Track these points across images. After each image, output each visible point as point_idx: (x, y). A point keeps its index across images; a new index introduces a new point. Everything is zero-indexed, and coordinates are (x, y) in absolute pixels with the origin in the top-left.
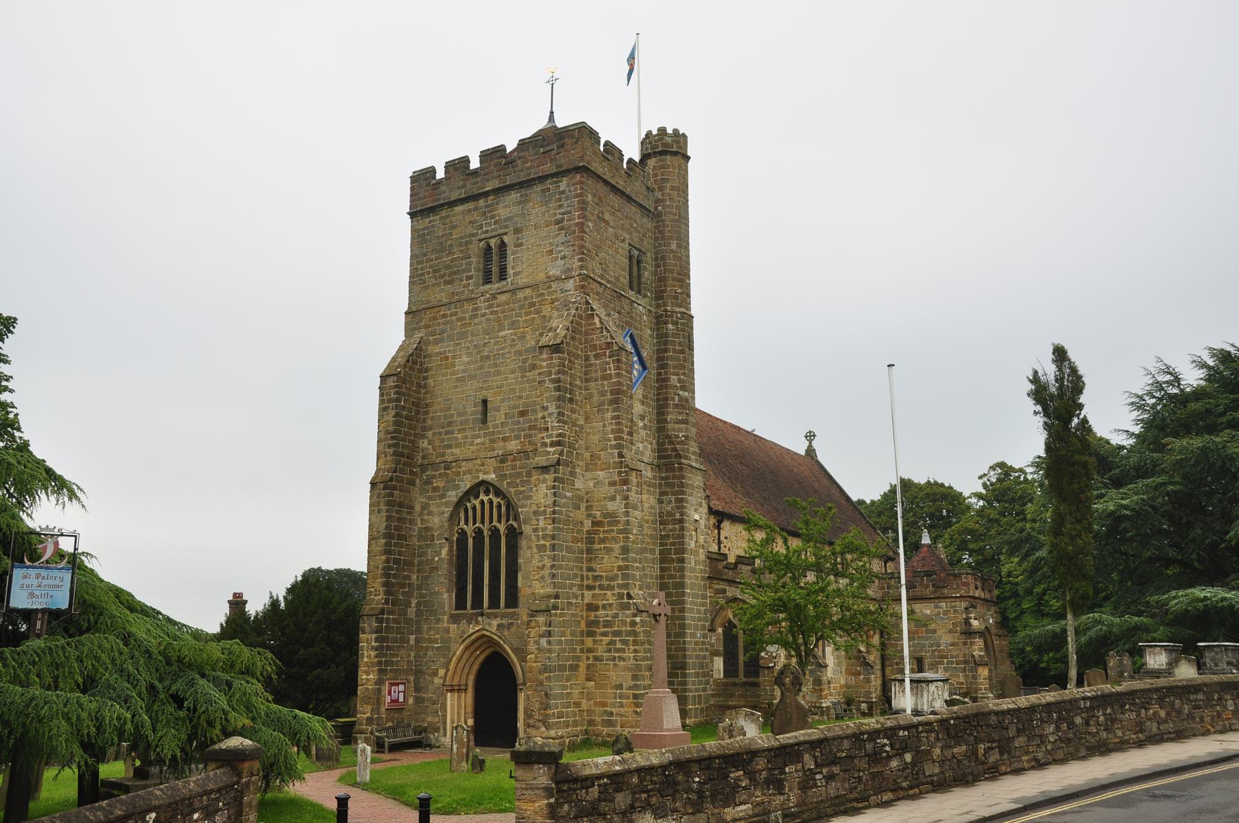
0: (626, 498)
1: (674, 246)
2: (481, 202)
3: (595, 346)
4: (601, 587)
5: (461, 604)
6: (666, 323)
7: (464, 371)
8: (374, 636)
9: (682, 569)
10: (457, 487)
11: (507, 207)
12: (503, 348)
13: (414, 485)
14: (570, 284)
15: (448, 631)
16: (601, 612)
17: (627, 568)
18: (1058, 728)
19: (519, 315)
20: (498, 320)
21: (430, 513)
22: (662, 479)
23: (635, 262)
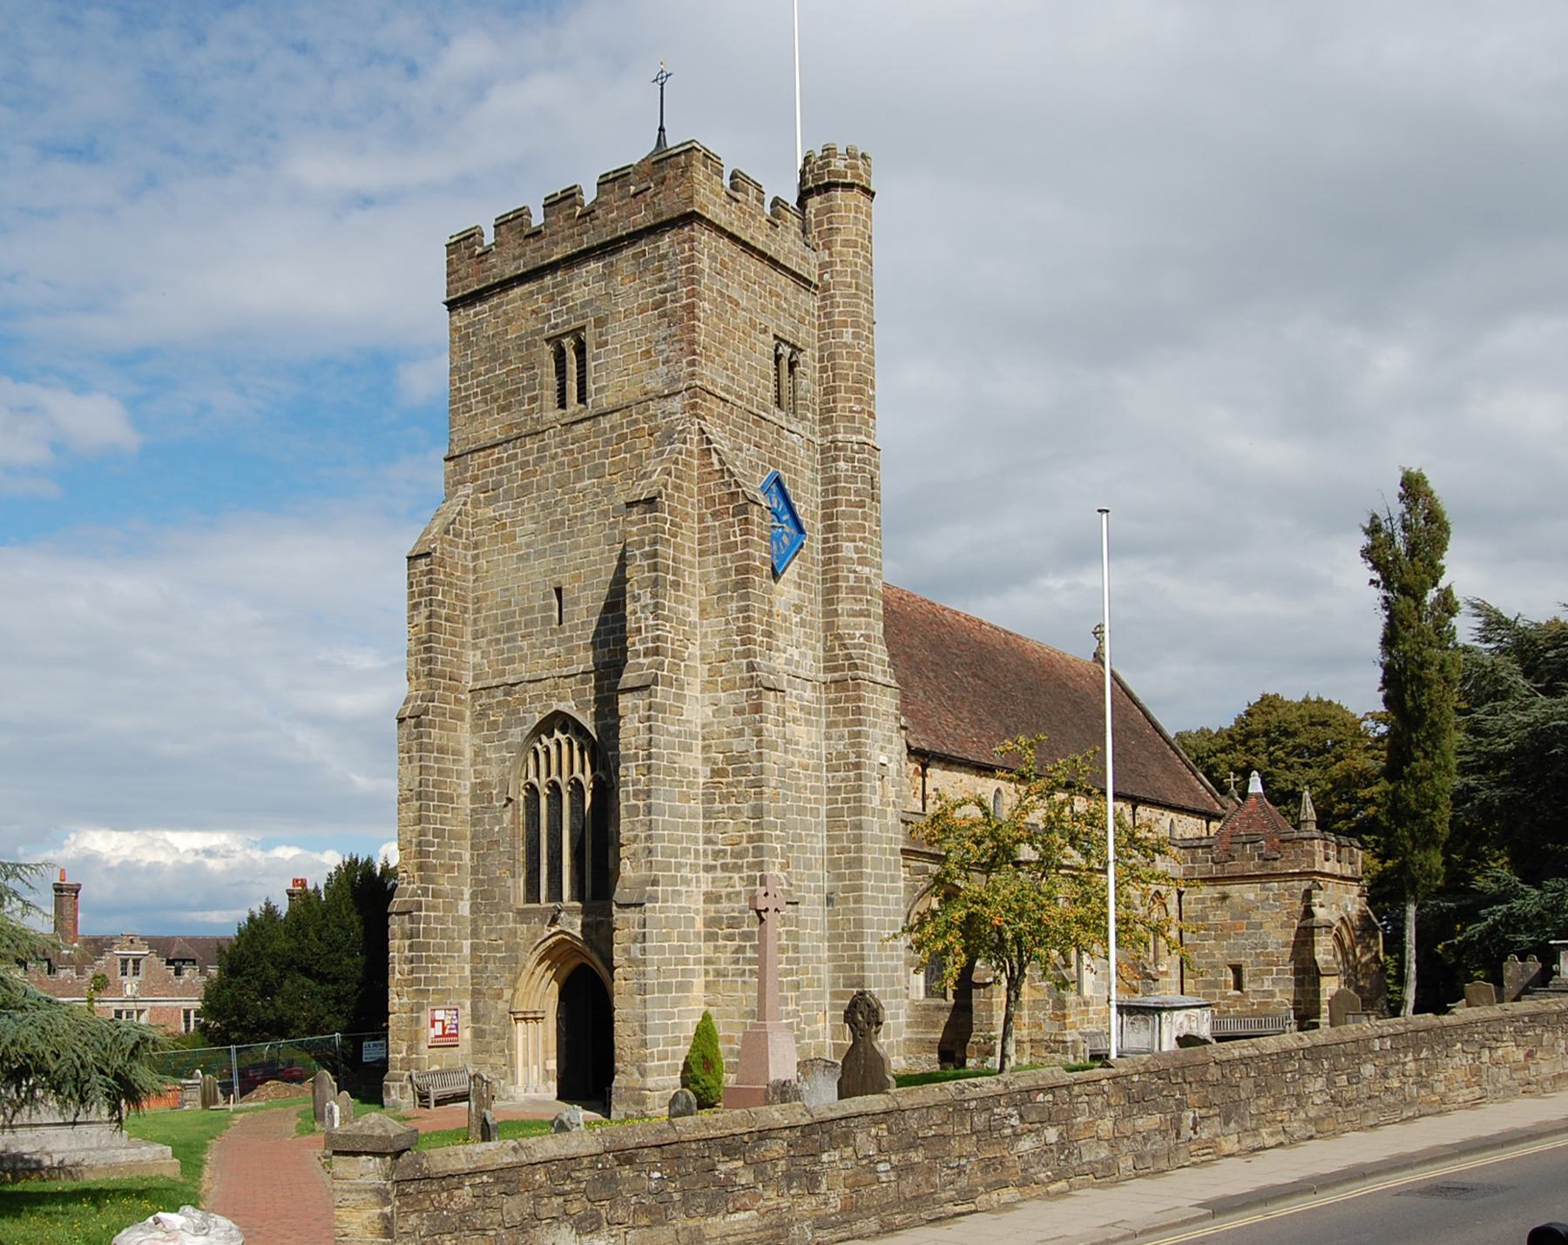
0: (759, 733)
1: (847, 336)
2: (548, 280)
3: (713, 498)
4: (725, 867)
5: (532, 893)
6: (835, 460)
7: (528, 545)
8: (407, 942)
9: (858, 839)
10: (522, 721)
11: (584, 284)
12: (582, 508)
13: (462, 719)
14: (676, 404)
15: (514, 933)
16: (725, 905)
17: (760, 838)
18: (1331, 1083)
19: (604, 455)
20: (574, 464)
21: (486, 761)
22: (830, 702)
23: (786, 361)
